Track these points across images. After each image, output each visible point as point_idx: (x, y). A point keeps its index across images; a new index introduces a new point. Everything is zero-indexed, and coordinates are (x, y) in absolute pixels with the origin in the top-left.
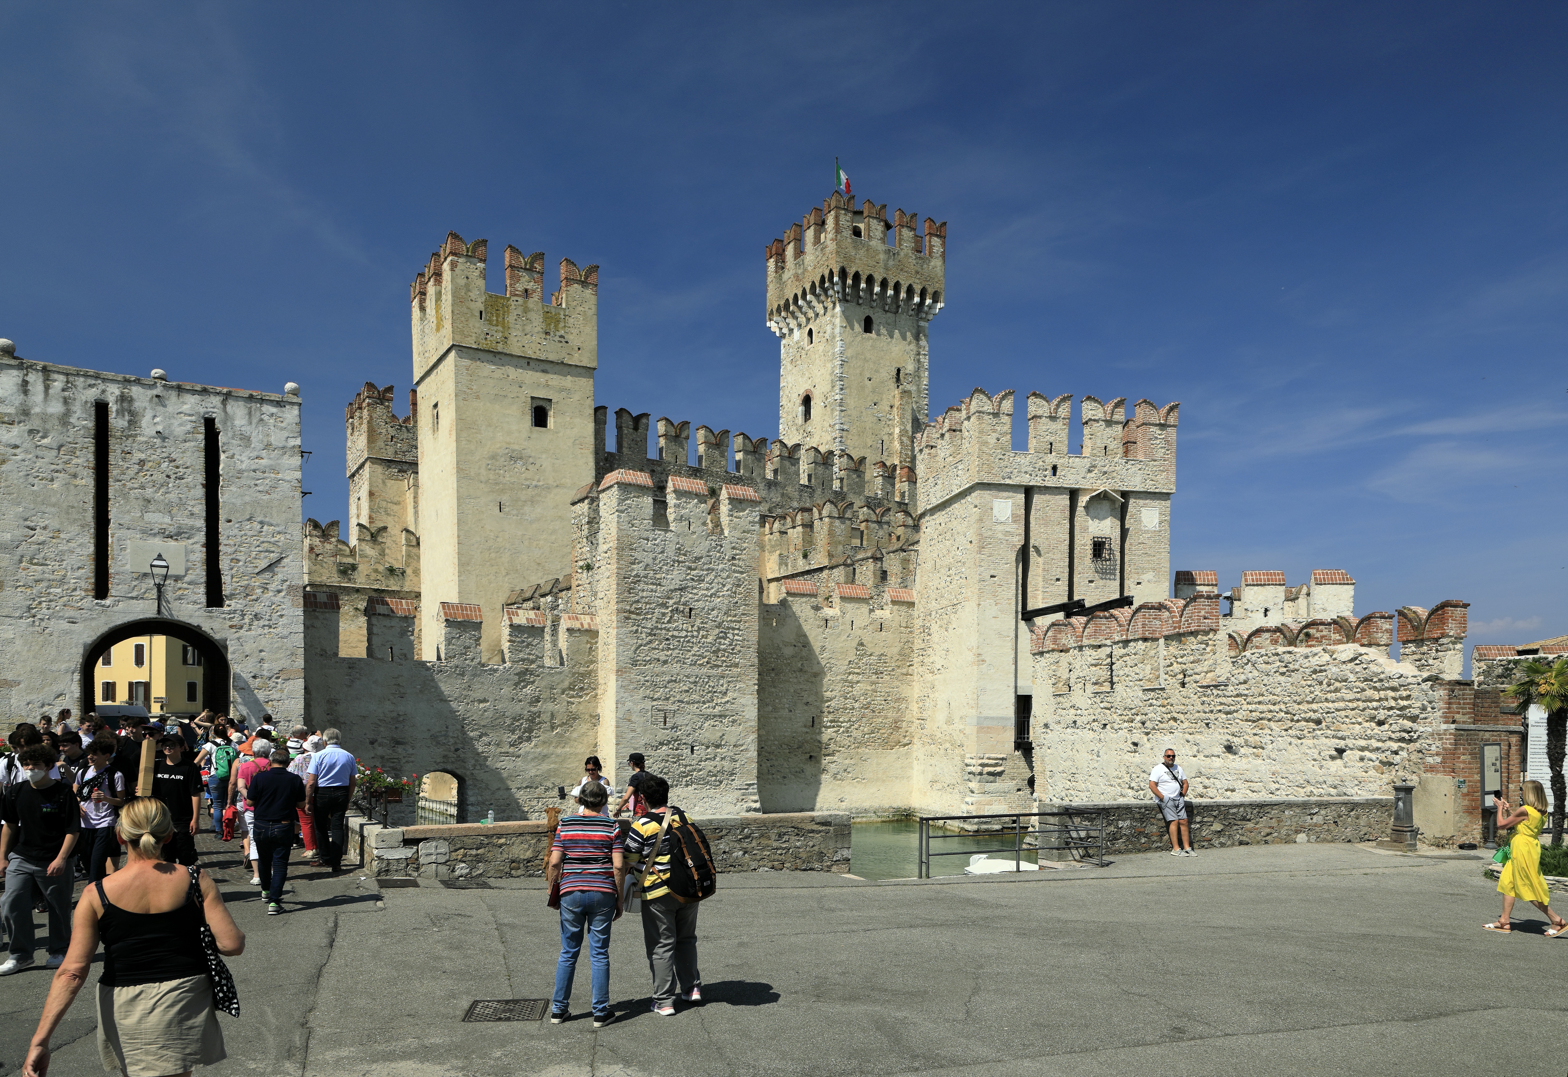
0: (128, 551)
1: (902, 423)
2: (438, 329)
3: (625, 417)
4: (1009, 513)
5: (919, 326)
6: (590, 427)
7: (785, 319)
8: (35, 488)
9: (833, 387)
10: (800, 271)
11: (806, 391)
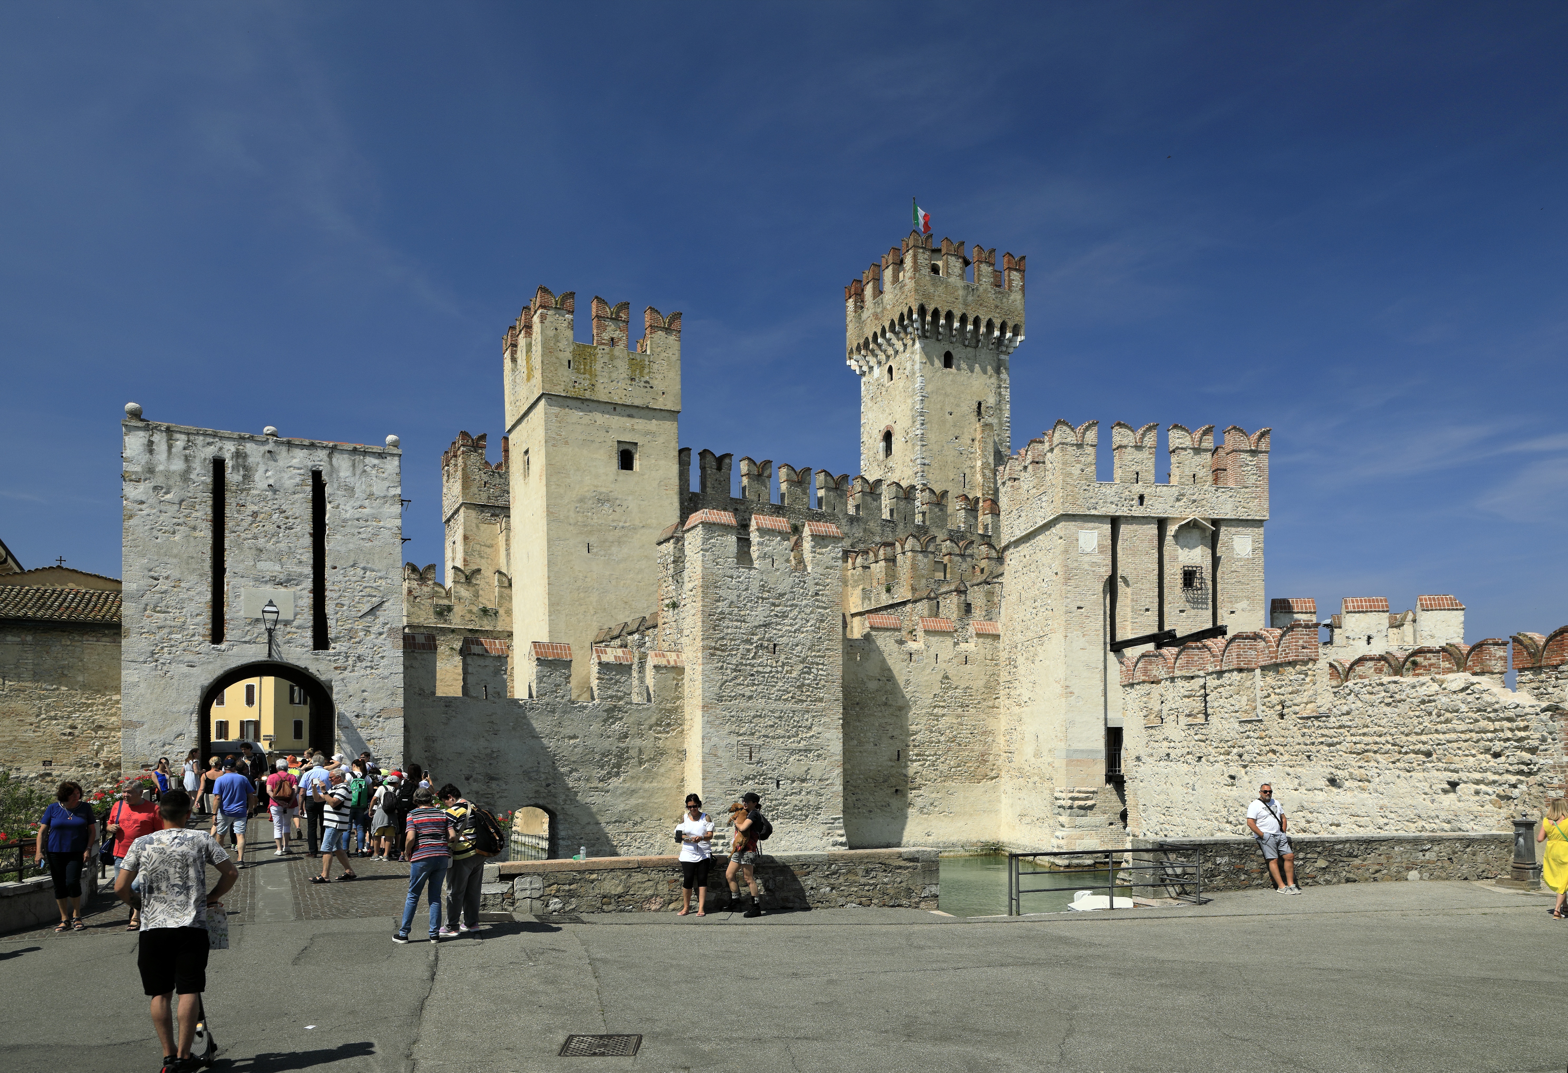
0: (242, 598)
1: (984, 456)
2: (528, 379)
3: (709, 458)
4: (1095, 544)
5: (999, 360)
6: (675, 468)
7: (865, 357)
8: (159, 541)
9: (914, 422)
10: (879, 310)
11: (887, 427)
